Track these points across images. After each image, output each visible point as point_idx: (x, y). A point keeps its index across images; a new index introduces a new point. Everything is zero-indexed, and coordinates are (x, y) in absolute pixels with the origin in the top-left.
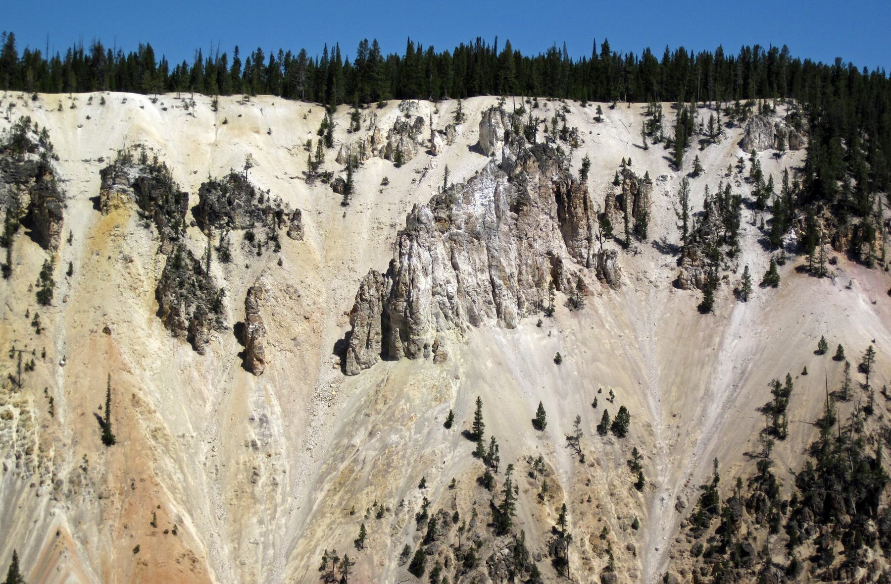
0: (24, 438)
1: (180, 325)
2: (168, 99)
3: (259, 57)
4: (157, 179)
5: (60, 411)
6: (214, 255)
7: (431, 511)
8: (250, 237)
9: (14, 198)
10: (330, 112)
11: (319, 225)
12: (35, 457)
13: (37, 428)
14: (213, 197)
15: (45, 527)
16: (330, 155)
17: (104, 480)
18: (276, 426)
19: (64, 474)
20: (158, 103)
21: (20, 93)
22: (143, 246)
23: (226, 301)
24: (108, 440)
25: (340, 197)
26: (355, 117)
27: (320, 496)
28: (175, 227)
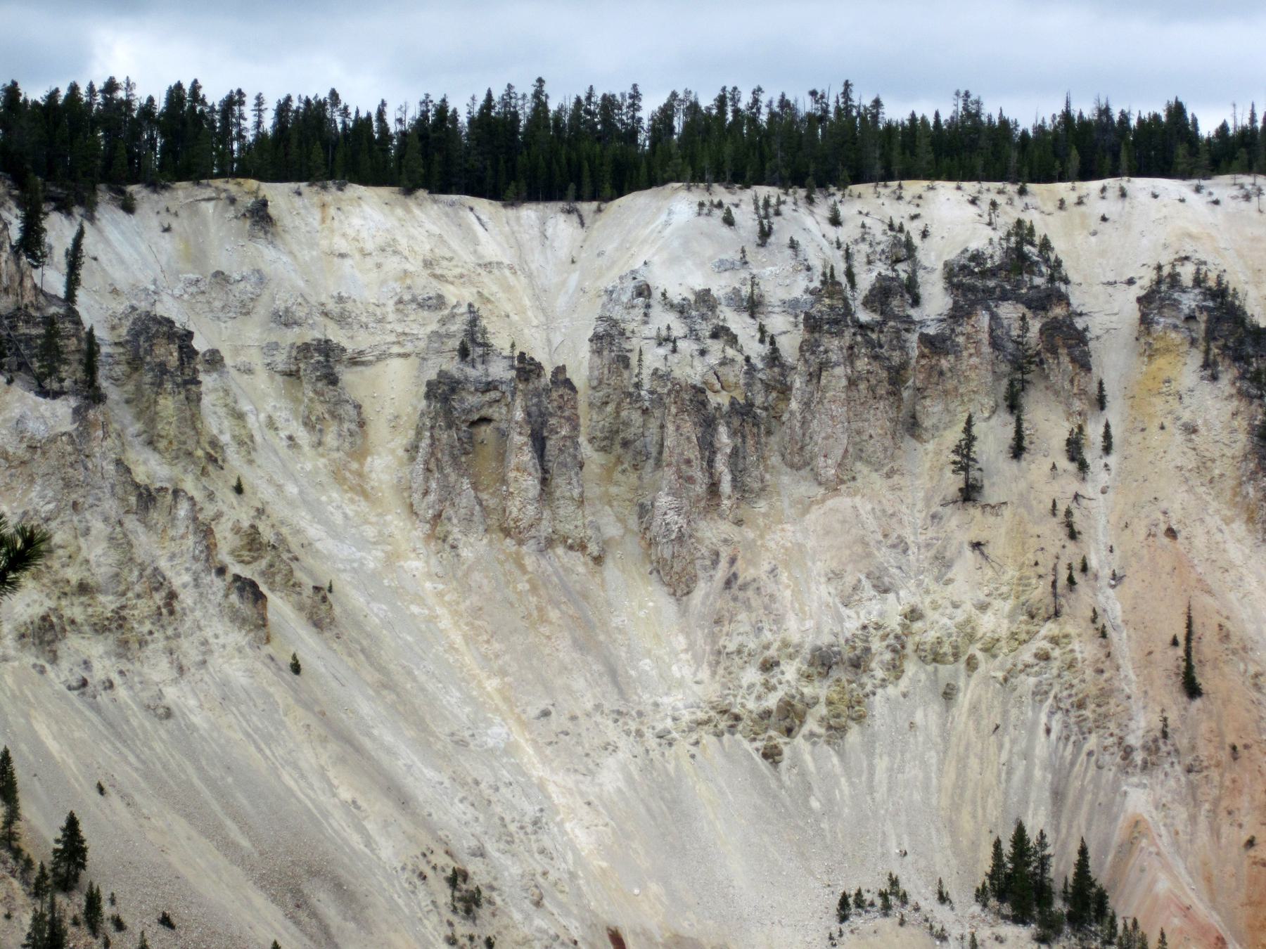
0: (1072, 686)
13: (1089, 673)
20: (1205, 192)
21: (999, 185)
24: (1192, 689)
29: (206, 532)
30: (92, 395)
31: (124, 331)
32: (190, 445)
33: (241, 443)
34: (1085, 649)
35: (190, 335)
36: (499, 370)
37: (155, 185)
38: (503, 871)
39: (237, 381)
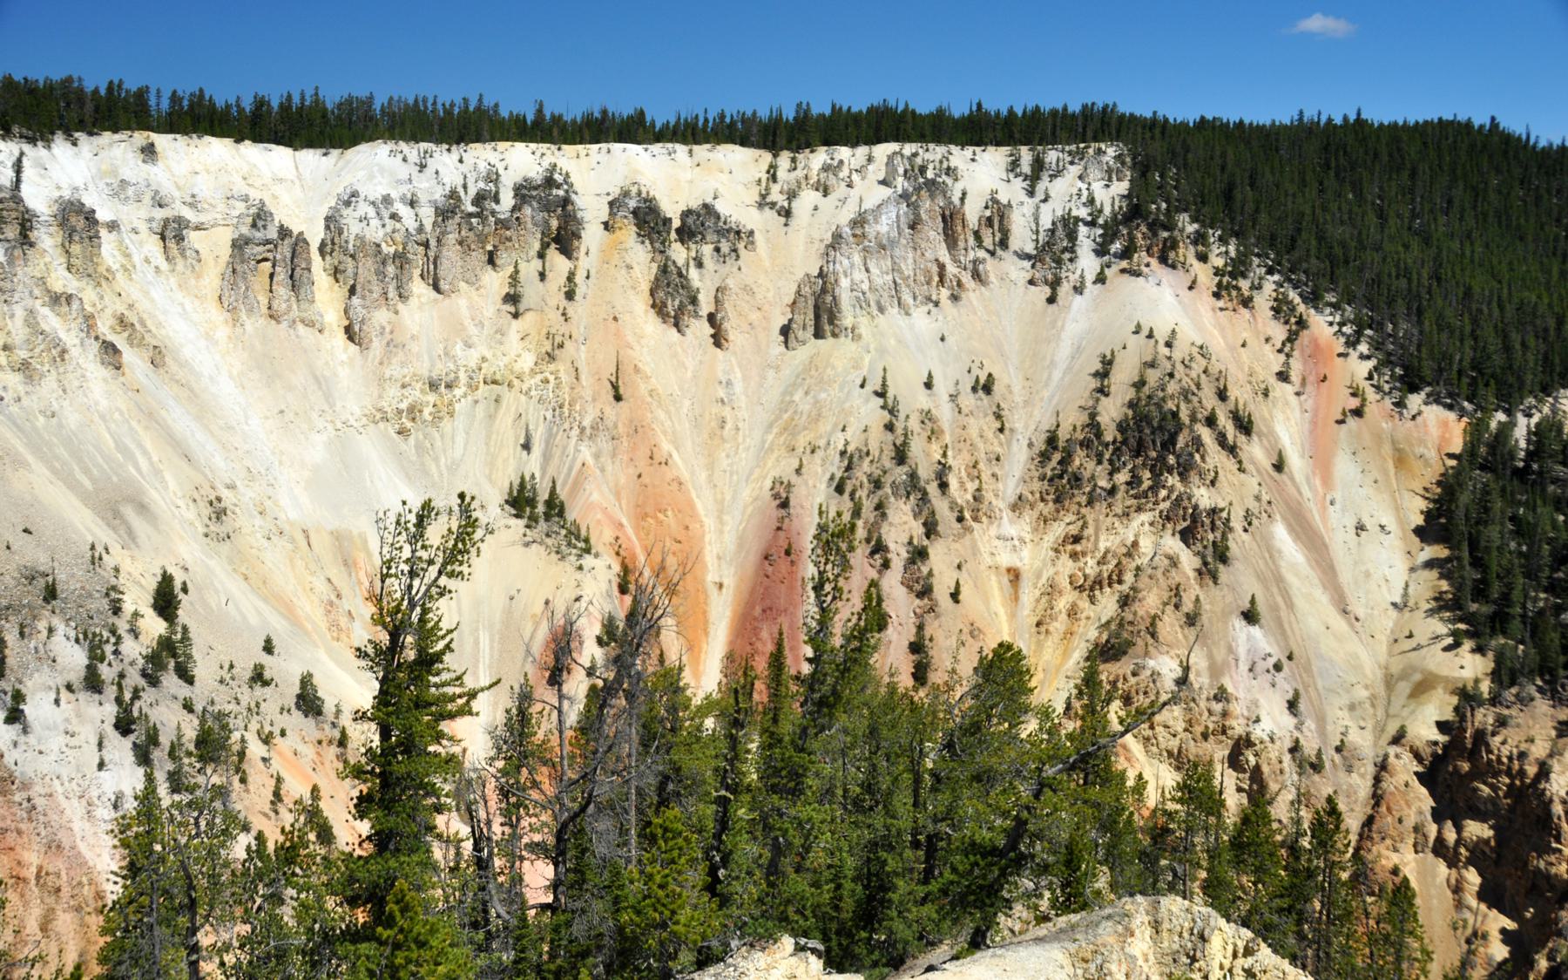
1: (668, 315)
2: (656, 148)
3: (722, 116)
4: (649, 208)
5: (583, 377)
6: (692, 263)
7: (850, 449)
8: (717, 250)
9: (547, 222)
10: (775, 156)
11: (768, 240)
12: (566, 410)
14: (690, 221)
15: (574, 459)
16: (775, 188)
17: (616, 427)
18: (738, 387)
19: (587, 423)
22: (640, 258)
23: (701, 297)
24: (618, 398)
25: (783, 220)
26: (794, 160)
27: (770, 437)
28: (663, 243)
29: (89, 321)
30: (25, 239)
31: (55, 209)
32: (90, 271)
33: (126, 270)
34: (566, 378)
35: (94, 211)
36: (272, 233)
37: (91, 134)
38: (241, 500)
39: (128, 239)
